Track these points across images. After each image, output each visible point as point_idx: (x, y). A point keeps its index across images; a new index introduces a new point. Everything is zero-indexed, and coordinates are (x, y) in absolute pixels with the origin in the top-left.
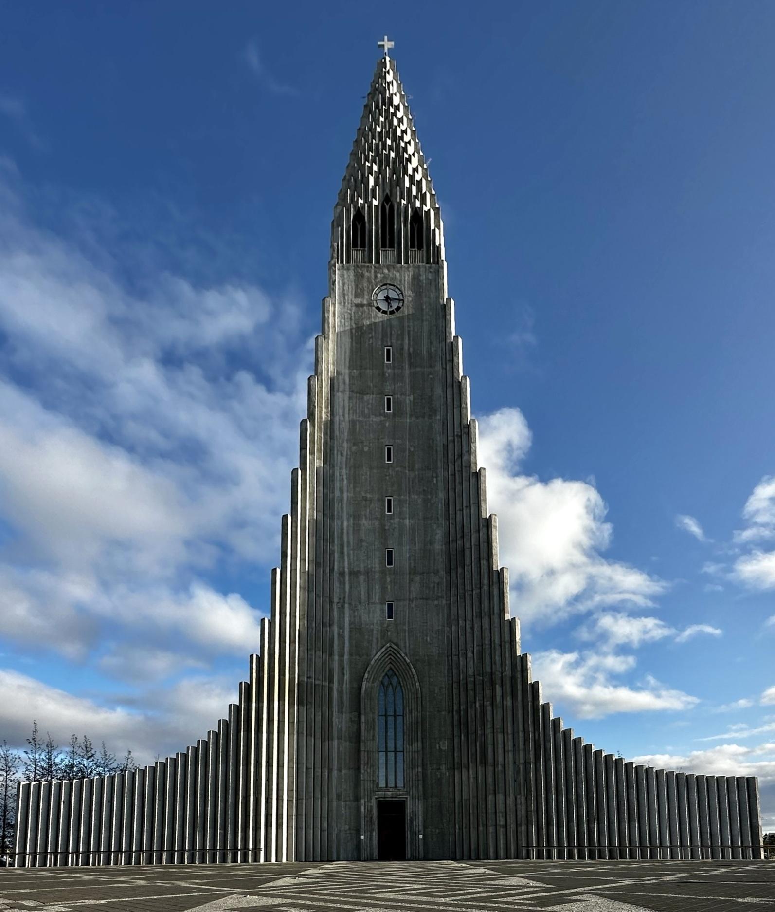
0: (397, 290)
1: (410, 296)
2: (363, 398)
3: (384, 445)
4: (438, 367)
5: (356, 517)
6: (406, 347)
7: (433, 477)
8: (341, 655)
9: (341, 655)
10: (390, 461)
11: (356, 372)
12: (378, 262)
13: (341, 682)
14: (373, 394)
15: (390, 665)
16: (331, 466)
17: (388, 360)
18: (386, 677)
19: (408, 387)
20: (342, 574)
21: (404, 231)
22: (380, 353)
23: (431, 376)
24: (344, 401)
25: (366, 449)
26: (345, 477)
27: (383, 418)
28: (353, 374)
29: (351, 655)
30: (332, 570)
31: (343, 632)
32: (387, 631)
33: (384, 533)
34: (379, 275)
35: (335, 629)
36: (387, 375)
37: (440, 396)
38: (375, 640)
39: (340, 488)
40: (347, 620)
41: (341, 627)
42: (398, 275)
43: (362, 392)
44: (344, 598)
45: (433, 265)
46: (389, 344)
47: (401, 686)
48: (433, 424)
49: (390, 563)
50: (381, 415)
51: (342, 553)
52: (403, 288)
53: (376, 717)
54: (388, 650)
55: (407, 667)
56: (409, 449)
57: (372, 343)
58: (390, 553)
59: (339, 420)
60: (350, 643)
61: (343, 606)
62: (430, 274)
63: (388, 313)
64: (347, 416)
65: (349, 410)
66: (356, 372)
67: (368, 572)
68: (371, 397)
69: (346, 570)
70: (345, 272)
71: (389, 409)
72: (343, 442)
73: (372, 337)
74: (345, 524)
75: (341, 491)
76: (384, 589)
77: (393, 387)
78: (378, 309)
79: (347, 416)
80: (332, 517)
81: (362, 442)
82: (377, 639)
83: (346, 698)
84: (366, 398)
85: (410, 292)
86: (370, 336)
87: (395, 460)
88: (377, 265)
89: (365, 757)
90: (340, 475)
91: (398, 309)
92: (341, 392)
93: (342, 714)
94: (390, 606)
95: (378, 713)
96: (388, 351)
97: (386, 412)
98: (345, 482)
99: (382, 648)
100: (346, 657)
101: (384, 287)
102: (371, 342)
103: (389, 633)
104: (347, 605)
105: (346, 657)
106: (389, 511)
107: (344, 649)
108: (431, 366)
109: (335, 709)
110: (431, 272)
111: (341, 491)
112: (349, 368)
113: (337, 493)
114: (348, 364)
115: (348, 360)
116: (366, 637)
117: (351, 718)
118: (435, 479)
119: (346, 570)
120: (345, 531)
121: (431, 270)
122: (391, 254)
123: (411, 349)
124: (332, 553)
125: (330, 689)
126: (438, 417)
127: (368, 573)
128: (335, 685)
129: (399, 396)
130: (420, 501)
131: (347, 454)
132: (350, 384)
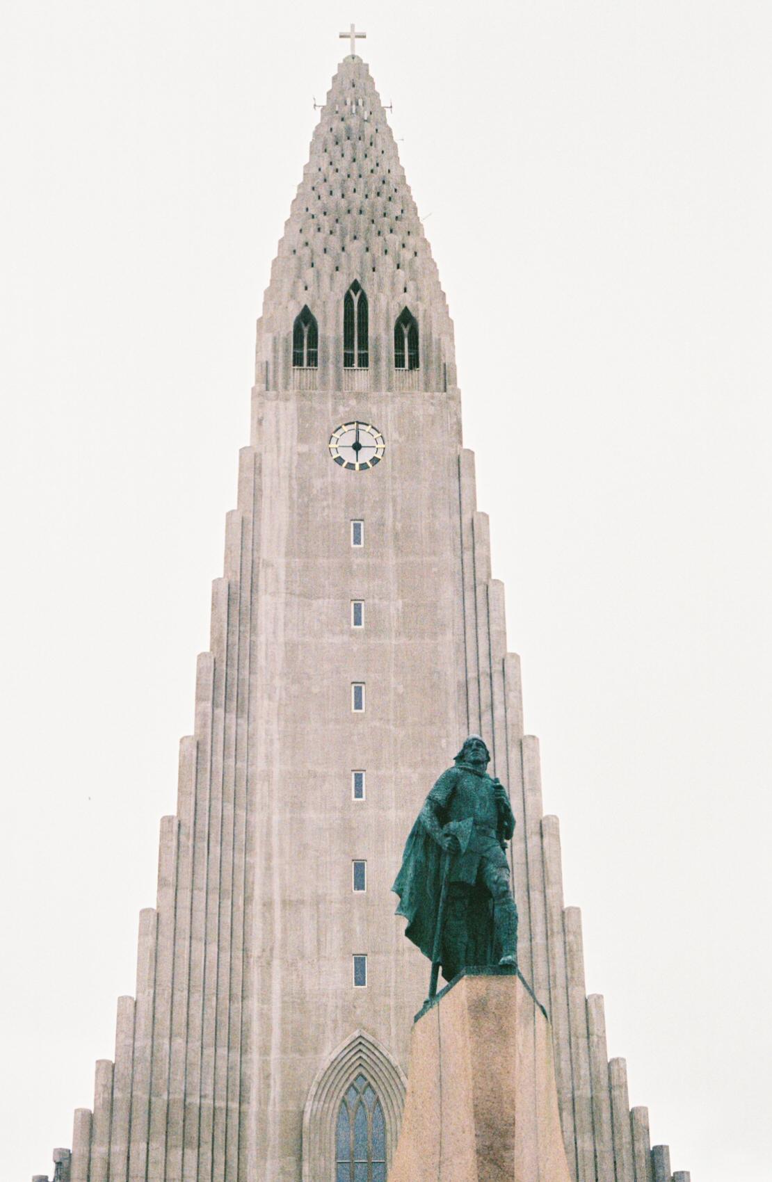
0: (373, 431)
1: (396, 441)
2: (310, 605)
3: (350, 683)
4: (448, 557)
5: (296, 805)
6: (389, 522)
7: (440, 737)
9: (265, 1051)
11: (297, 562)
12: (338, 387)
14: (329, 598)
15: (360, 1070)
16: (251, 719)
17: (357, 541)
18: (353, 1091)
19: (393, 588)
20: (268, 905)
22: (343, 531)
23: (435, 569)
24: (276, 609)
25: (315, 690)
26: (276, 736)
27: (346, 638)
28: (293, 565)
29: (284, 1051)
30: (247, 900)
31: (270, 1010)
32: (355, 1007)
33: (348, 831)
34: (341, 409)
35: (254, 1004)
36: (355, 567)
37: (453, 601)
38: (330, 1024)
39: (267, 757)
40: (276, 987)
41: (265, 999)
42: (374, 410)
43: (308, 595)
44: (272, 950)
45: (437, 394)
47: (381, 1111)
48: (439, 649)
49: (360, 884)
50: (342, 632)
51: (268, 868)
52: (384, 428)
53: (333, 1165)
54: (357, 1043)
55: (393, 1073)
56: (395, 689)
57: (328, 516)
58: (359, 868)
59: (267, 640)
60: (284, 1033)
63: (357, 467)
64: (281, 634)
65: (285, 624)
66: (297, 562)
67: (318, 901)
68: (327, 600)
69: (277, 898)
70: (281, 404)
71: (358, 622)
72: (272, 677)
73: (328, 506)
74: (276, 818)
75: (269, 759)
76: (348, 932)
77: (366, 586)
78: (339, 461)
79: (281, 634)
80: (249, 807)
81: (309, 678)
82: (335, 1021)
83: (274, 1131)
84: (316, 603)
85: (396, 436)
86: (325, 503)
87: (370, 709)
88: (339, 393)
90: (266, 735)
91: (375, 461)
92: (270, 594)
93: (266, 1160)
94: (360, 962)
95: (336, 1158)
96: (357, 527)
98: (277, 745)
99: (344, 1037)
100: (275, 1055)
102: (325, 514)
103: (358, 1011)
104: (276, 963)
105: (275, 1055)
106: (359, 795)
107: (269, 1041)
108: (434, 553)
109: (252, 1153)
110: (432, 404)
111: (269, 759)
112: (287, 554)
113: (260, 765)
114: (283, 550)
115: (283, 544)
116: (314, 1018)
117: (282, 1168)
118: (444, 741)
119: (277, 898)
120: (275, 830)
121: (434, 401)
122: (361, 378)
123: (399, 526)
126: (449, 637)
127: (318, 904)
128: (253, 1108)
129: (377, 601)
130: (415, 777)
131: (280, 699)
132: (286, 582)
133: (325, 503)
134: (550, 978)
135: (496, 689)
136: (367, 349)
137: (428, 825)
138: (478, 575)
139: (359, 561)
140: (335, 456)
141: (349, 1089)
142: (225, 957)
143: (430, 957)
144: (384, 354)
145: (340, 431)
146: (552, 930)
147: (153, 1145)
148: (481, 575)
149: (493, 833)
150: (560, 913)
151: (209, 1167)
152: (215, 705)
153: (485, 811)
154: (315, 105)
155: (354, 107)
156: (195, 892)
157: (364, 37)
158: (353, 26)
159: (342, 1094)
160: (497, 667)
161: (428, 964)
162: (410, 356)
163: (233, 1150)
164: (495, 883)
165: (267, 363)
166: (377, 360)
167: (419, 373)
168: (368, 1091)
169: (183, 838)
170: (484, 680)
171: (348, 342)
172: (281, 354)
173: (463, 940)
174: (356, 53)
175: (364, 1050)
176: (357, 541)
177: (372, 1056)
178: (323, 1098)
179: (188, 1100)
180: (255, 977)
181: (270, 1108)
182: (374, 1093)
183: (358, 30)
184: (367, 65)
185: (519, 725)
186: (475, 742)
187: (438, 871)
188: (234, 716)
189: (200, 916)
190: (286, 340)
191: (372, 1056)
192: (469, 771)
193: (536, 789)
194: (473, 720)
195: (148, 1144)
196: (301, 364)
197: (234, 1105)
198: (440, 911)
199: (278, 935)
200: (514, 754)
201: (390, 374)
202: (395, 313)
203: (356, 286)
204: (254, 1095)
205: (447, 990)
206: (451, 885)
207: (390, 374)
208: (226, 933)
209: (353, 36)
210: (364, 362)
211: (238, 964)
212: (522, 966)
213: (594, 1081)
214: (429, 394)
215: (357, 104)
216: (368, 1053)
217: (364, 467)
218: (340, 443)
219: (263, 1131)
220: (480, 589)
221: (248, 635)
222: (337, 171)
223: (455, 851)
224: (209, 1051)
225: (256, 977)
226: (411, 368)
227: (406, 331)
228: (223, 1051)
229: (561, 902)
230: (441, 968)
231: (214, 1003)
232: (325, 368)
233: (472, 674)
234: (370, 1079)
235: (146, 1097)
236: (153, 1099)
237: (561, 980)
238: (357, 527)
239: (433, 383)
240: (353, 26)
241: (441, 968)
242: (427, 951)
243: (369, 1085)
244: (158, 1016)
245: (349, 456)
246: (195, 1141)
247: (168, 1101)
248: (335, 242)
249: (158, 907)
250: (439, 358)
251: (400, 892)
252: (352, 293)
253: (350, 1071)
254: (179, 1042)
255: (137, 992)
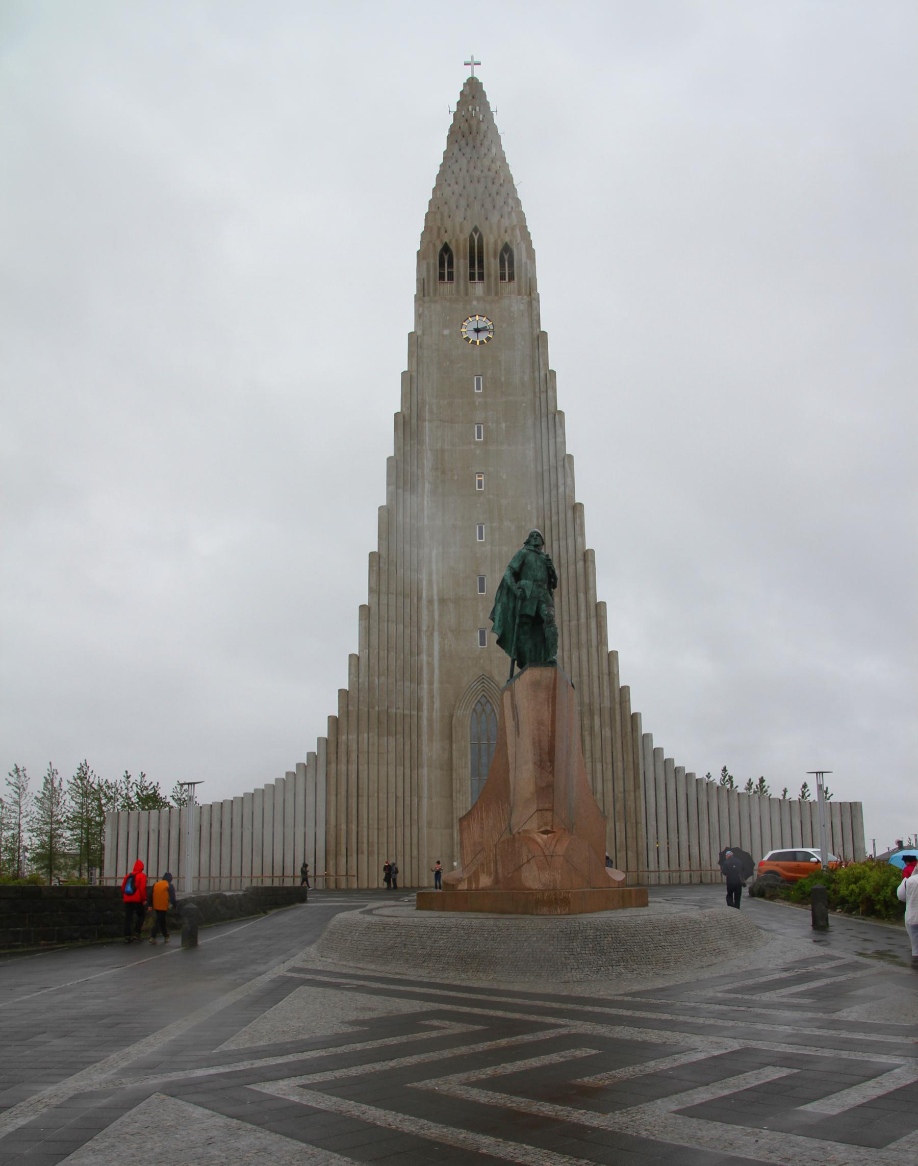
8: (431, 683)
9: (431, 683)
10: (482, 488)
13: (431, 709)
15: (483, 693)
17: (478, 388)
20: (430, 602)
21: (492, 264)
23: (524, 405)
29: (441, 682)
30: (419, 598)
31: (433, 660)
35: (424, 657)
40: (436, 647)
41: (430, 655)
44: (433, 626)
46: (479, 374)
49: (482, 590)
53: (469, 745)
58: (482, 580)
61: (432, 634)
62: (521, 305)
63: (478, 343)
69: (435, 597)
71: (479, 437)
86: (459, 365)
89: (456, 784)
95: (471, 741)
96: (478, 380)
97: (477, 440)
100: (436, 685)
101: (474, 318)
103: (482, 661)
104: (436, 634)
105: (436, 685)
107: (433, 677)
109: (425, 737)
110: (522, 303)
118: (529, 506)
119: (435, 597)
121: (523, 302)
122: (479, 288)
124: (419, 582)
125: (419, 718)
128: (425, 714)
133: (459, 365)
134: (589, 641)
135: (560, 476)
136: (483, 269)
137: (509, 582)
138: (550, 408)
139: (480, 400)
140: (464, 337)
141: (477, 703)
142: (407, 631)
143: (510, 656)
144: (493, 273)
145: (467, 321)
146: (590, 615)
147: (371, 734)
148: (551, 408)
149: (546, 586)
150: (594, 605)
151: (402, 747)
152: (397, 488)
153: (541, 574)
154: (450, 111)
155: (474, 112)
156: (390, 595)
157: (480, 64)
158: (472, 57)
159: (473, 706)
160: (560, 463)
161: (510, 659)
162: (509, 273)
163: (414, 737)
164: (546, 615)
165: (423, 279)
166: (489, 276)
167: (514, 285)
168: (488, 705)
169: (382, 565)
170: (553, 471)
171: (472, 265)
172: (432, 273)
173: (528, 646)
174: (475, 76)
175: (486, 682)
176: (478, 388)
177: (490, 685)
178: (463, 708)
179: (389, 711)
180: (424, 641)
181: (434, 714)
182: (491, 705)
183: (476, 60)
184: (482, 83)
185: (573, 497)
186: (535, 534)
187: (514, 608)
188: (409, 493)
189: (392, 608)
190: (435, 264)
191: (490, 685)
192: (532, 550)
193: (583, 535)
194: (546, 495)
195: (368, 734)
196: (444, 280)
197: (415, 713)
198: (516, 630)
199: (436, 617)
200: (570, 514)
201: (496, 285)
202: (500, 248)
203: (476, 230)
204: (425, 707)
205: (519, 675)
206: (521, 616)
207: (496, 285)
208: (407, 619)
209: (472, 64)
210: (481, 277)
211: (415, 634)
212: (559, 662)
213: (612, 699)
214: (520, 297)
215: (476, 110)
216: (487, 683)
217: (482, 342)
218: (467, 329)
219: (431, 725)
220: (550, 416)
221: (416, 446)
222: (464, 155)
223: (524, 599)
224: (400, 683)
225: (425, 641)
226: (509, 281)
227: (506, 257)
228: (407, 683)
229: (596, 600)
230: (516, 662)
231: (402, 657)
232: (458, 282)
233: (545, 467)
234: (488, 698)
235: (366, 709)
236: (370, 710)
237: (594, 643)
238: (478, 380)
239: (523, 291)
240: (472, 57)
241: (516, 662)
242: (508, 651)
243: (488, 701)
244: (371, 665)
245: (473, 337)
246: (394, 732)
247: (378, 711)
248: (463, 202)
249: (369, 603)
250: (526, 275)
251: (493, 620)
252: (474, 235)
253: (478, 693)
254: (383, 679)
255: (359, 652)
